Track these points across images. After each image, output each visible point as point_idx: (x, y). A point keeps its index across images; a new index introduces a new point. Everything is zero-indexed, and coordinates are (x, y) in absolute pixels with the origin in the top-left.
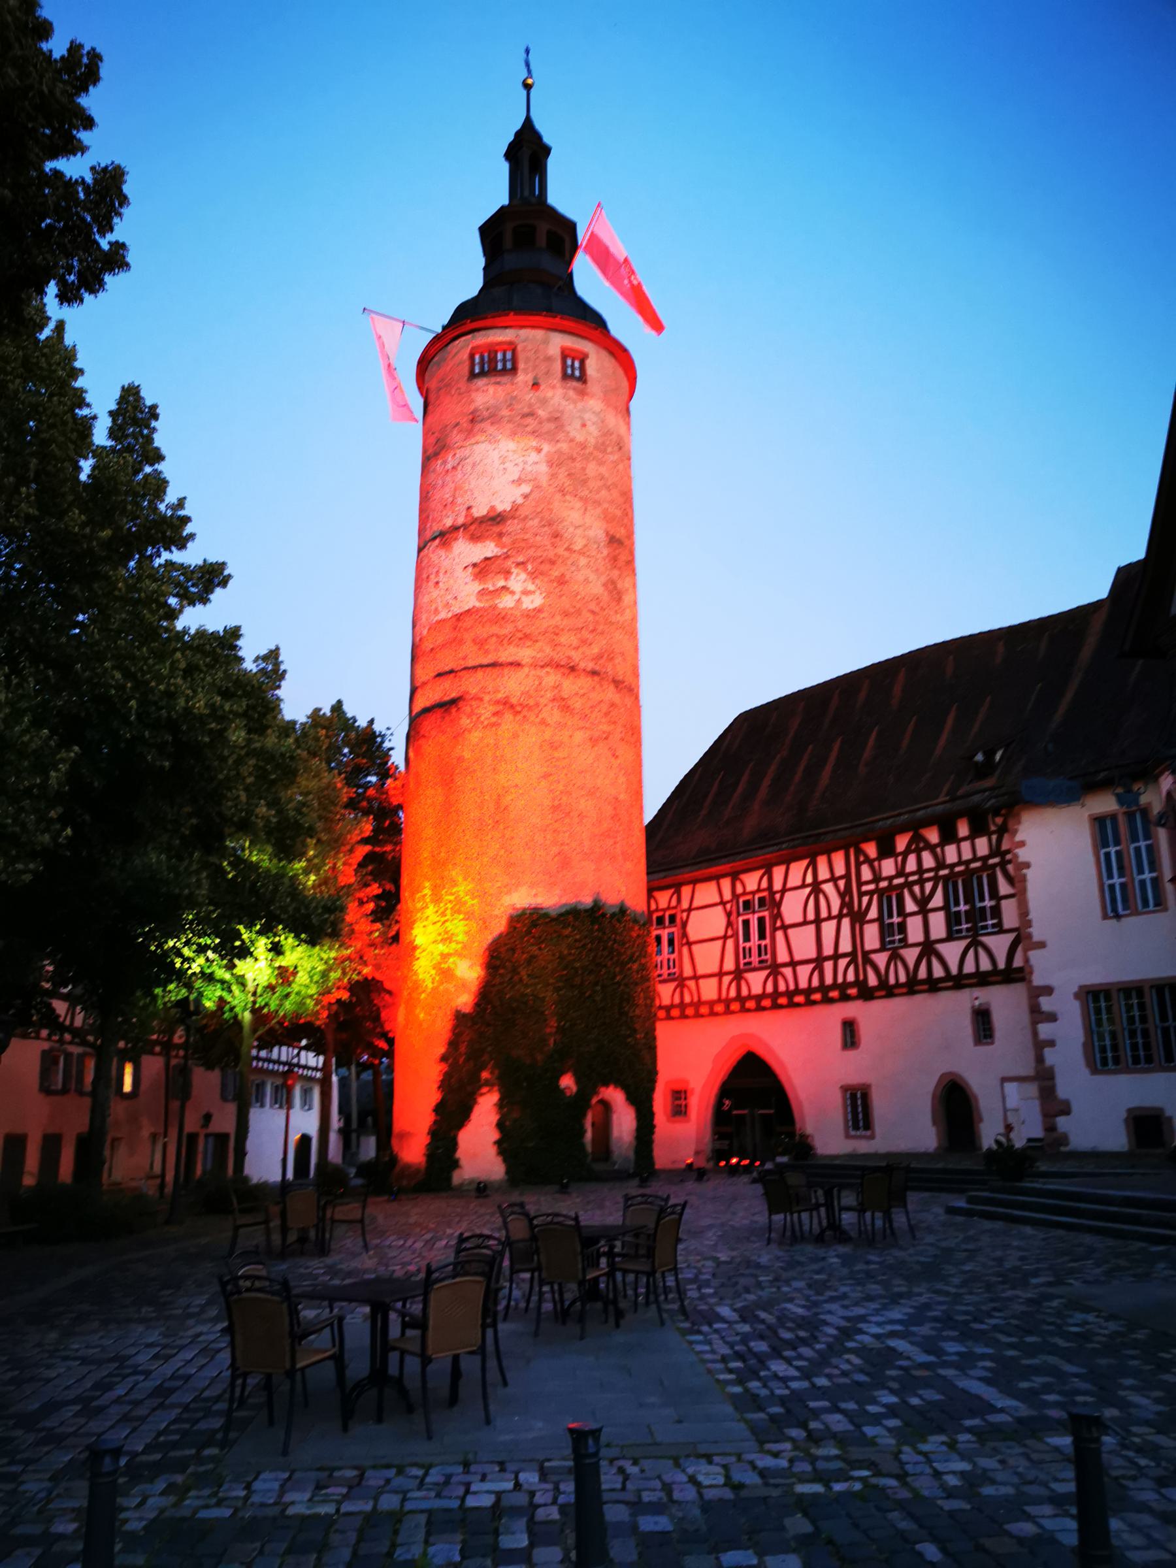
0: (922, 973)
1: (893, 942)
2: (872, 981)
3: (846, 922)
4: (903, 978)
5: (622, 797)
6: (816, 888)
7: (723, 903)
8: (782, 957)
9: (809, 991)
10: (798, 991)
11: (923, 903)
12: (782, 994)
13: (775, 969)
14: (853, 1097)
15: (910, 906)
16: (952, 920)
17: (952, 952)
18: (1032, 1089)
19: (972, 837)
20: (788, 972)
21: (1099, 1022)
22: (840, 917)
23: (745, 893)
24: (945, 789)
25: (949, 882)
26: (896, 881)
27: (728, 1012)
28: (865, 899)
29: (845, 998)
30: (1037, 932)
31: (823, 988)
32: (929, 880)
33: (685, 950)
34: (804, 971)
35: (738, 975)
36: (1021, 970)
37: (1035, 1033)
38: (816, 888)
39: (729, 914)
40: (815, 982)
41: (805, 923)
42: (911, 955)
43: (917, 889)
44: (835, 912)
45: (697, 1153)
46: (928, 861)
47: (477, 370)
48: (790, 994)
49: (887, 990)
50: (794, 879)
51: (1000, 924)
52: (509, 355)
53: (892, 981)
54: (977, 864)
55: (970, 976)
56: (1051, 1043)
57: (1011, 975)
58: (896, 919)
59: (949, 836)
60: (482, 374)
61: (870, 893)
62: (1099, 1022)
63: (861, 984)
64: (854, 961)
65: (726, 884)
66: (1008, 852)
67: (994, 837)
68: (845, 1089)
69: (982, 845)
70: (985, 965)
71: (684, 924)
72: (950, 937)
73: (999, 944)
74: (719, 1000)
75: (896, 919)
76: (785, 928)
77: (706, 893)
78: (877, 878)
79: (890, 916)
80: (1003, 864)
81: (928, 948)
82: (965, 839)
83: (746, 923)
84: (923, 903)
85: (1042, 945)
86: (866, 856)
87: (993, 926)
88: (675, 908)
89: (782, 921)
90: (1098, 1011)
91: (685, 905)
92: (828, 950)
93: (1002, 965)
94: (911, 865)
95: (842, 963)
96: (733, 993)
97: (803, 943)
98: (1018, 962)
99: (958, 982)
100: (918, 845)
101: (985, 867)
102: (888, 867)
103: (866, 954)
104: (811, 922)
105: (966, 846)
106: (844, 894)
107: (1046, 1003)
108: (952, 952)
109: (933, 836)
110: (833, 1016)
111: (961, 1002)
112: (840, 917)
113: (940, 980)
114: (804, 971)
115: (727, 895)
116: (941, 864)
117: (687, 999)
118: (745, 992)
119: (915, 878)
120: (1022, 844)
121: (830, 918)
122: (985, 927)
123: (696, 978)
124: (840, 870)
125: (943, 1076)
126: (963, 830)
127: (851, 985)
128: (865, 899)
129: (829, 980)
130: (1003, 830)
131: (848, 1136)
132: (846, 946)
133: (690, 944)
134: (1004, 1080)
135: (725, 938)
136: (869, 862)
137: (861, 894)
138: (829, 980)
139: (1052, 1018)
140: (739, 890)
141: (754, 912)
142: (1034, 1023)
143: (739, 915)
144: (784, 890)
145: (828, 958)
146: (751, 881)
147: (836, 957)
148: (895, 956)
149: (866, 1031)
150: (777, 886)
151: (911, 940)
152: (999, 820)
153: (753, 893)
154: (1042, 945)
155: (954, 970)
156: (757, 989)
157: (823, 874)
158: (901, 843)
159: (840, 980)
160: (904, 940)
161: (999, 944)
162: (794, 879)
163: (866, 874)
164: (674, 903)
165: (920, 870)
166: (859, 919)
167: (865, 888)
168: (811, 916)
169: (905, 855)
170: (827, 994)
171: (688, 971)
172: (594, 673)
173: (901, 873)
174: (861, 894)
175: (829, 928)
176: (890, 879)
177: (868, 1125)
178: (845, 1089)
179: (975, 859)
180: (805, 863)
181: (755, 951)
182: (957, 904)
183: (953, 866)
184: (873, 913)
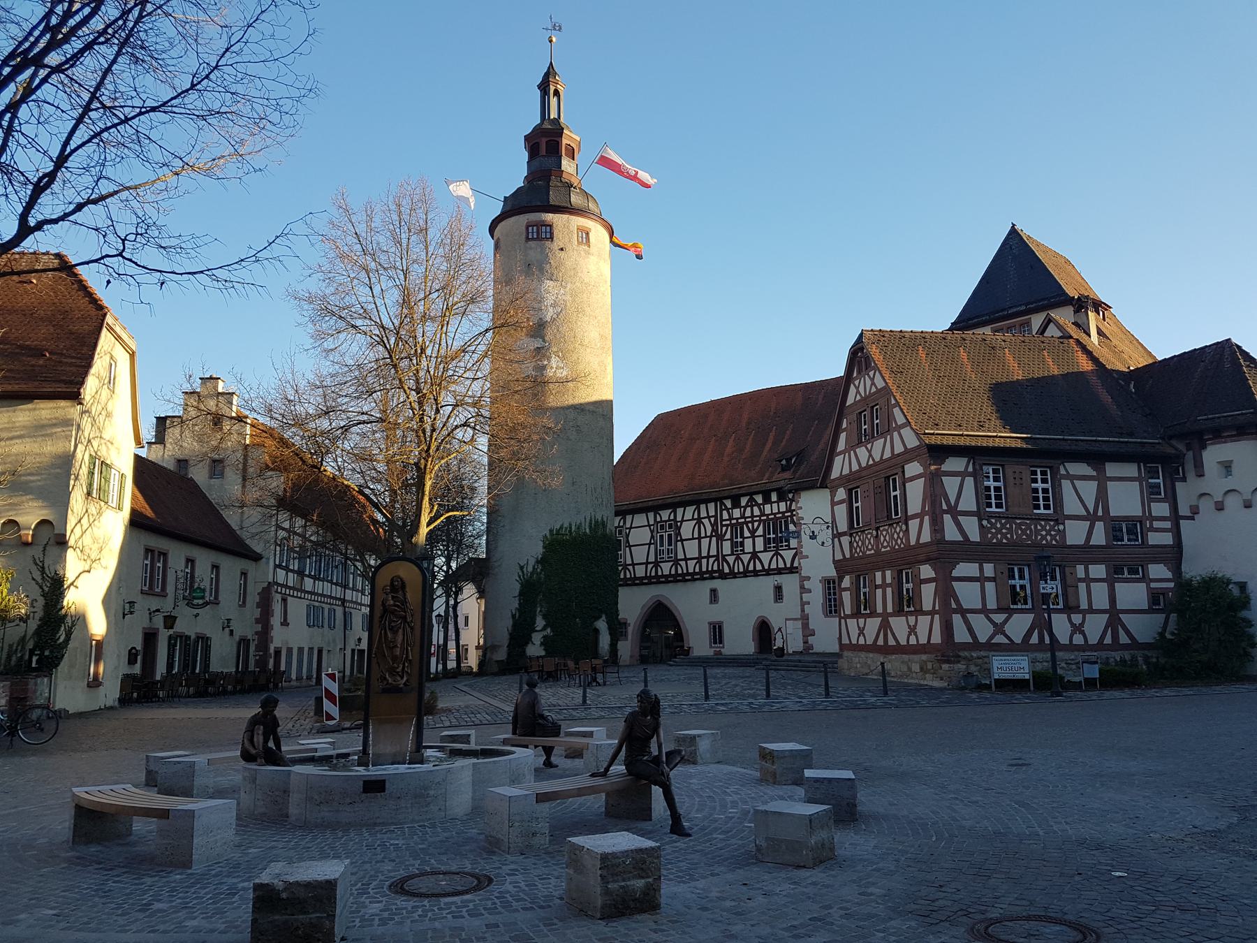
0: (751, 568)
1: (737, 551)
2: (727, 570)
3: (714, 539)
4: (741, 570)
5: (606, 477)
6: (699, 521)
7: (649, 526)
8: (681, 556)
9: (694, 573)
10: (688, 574)
11: (753, 532)
12: (680, 575)
13: (676, 562)
14: (714, 627)
15: (747, 534)
16: (767, 542)
17: (766, 557)
18: (799, 624)
19: (778, 502)
20: (683, 563)
21: (830, 594)
22: (711, 537)
23: (661, 521)
24: (765, 478)
25: (766, 523)
26: (740, 521)
27: (650, 583)
28: (724, 528)
29: (714, 578)
30: (805, 551)
31: (701, 572)
32: (756, 521)
33: (627, 549)
34: (691, 564)
35: (656, 564)
36: (797, 568)
37: (801, 599)
38: (699, 521)
39: (652, 532)
40: (697, 570)
41: (693, 539)
42: (746, 558)
43: (750, 525)
44: (708, 534)
45: (631, 657)
46: (757, 512)
47: (530, 237)
48: (683, 575)
49: (733, 575)
50: (688, 515)
51: (788, 545)
52: (548, 228)
53: (736, 571)
54: (780, 515)
55: (773, 570)
56: (808, 603)
57: (792, 570)
58: (739, 540)
59: (767, 500)
60: (533, 239)
61: (727, 526)
62: (830, 594)
63: (720, 571)
64: (717, 559)
65: (651, 515)
66: (794, 510)
67: (788, 503)
68: (710, 624)
69: (783, 507)
70: (781, 565)
71: (628, 536)
72: (765, 551)
73: (788, 555)
74: (646, 577)
75: (739, 540)
76: (682, 540)
77: (640, 519)
78: (731, 519)
79: (736, 538)
80: (792, 516)
81: (754, 555)
82: (774, 502)
83: (662, 537)
84: (753, 532)
85: (807, 557)
86: (725, 506)
87: (786, 546)
88: (622, 527)
89: (681, 537)
90: (829, 588)
91: (628, 526)
92: (704, 554)
93: (788, 565)
94: (748, 513)
95: (711, 560)
96: (653, 574)
97: (692, 549)
98: (796, 564)
99: (768, 572)
100: (752, 503)
101: (784, 517)
102: (737, 513)
103: (724, 556)
104: (696, 539)
105: (775, 505)
106: (714, 525)
107: (807, 584)
108: (766, 557)
109: (759, 499)
110: (706, 586)
111: (769, 582)
112: (711, 537)
113: (760, 571)
114: (691, 564)
115: (652, 522)
116: (763, 514)
117: (628, 576)
118: (660, 573)
119: (750, 519)
120: (801, 508)
121: (706, 537)
122: (782, 546)
123: (633, 565)
124: (712, 513)
125: (759, 617)
126: (774, 497)
127: (715, 572)
128: (724, 528)
129: (704, 569)
130: (792, 500)
131: (711, 647)
132: (713, 552)
133: (630, 547)
134: (786, 619)
135: (650, 544)
136: (727, 509)
137: (722, 526)
138: (704, 569)
139: (809, 591)
140: (658, 519)
141: (666, 531)
142: (801, 593)
143: (658, 532)
144: (683, 521)
145: (704, 557)
146: (665, 515)
147: (708, 557)
148: (738, 558)
149: (720, 594)
150: (679, 519)
151: (746, 551)
152: (790, 496)
153: (664, 521)
154: (807, 557)
155: (766, 567)
156: (666, 572)
157: (703, 514)
158: (744, 501)
159: (710, 569)
160: (743, 550)
161: (788, 555)
162: (688, 515)
163: (725, 516)
164: (621, 524)
165: (752, 516)
166: (720, 538)
167: (724, 523)
168: (696, 535)
169: (745, 508)
170: (702, 576)
171: (629, 562)
172: (593, 412)
173: (743, 516)
174: (722, 526)
175: (705, 542)
176: (737, 519)
177: (721, 642)
178: (710, 624)
179: (779, 513)
180: (695, 507)
181: (666, 552)
182: (769, 534)
183: (768, 515)
184: (728, 536)
